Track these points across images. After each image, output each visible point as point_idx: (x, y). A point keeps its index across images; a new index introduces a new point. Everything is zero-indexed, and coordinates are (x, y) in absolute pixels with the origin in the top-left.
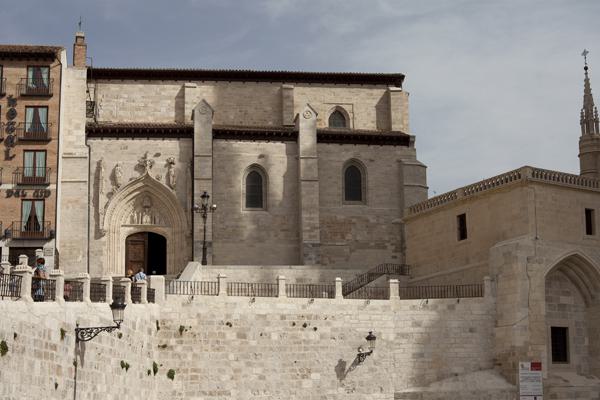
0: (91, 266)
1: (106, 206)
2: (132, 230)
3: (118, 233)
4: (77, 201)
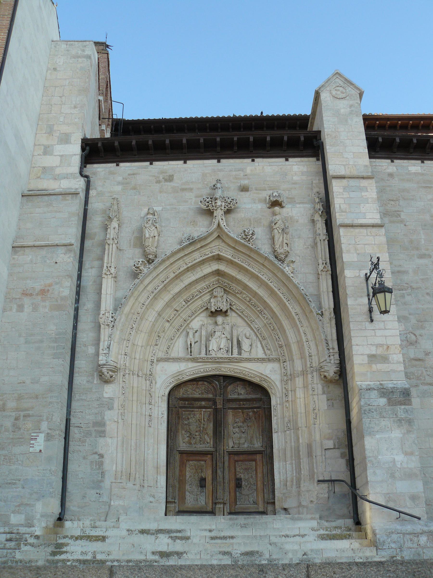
0: (71, 467)
1: (118, 306)
2: (190, 370)
3: (150, 377)
4: (43, 292)
